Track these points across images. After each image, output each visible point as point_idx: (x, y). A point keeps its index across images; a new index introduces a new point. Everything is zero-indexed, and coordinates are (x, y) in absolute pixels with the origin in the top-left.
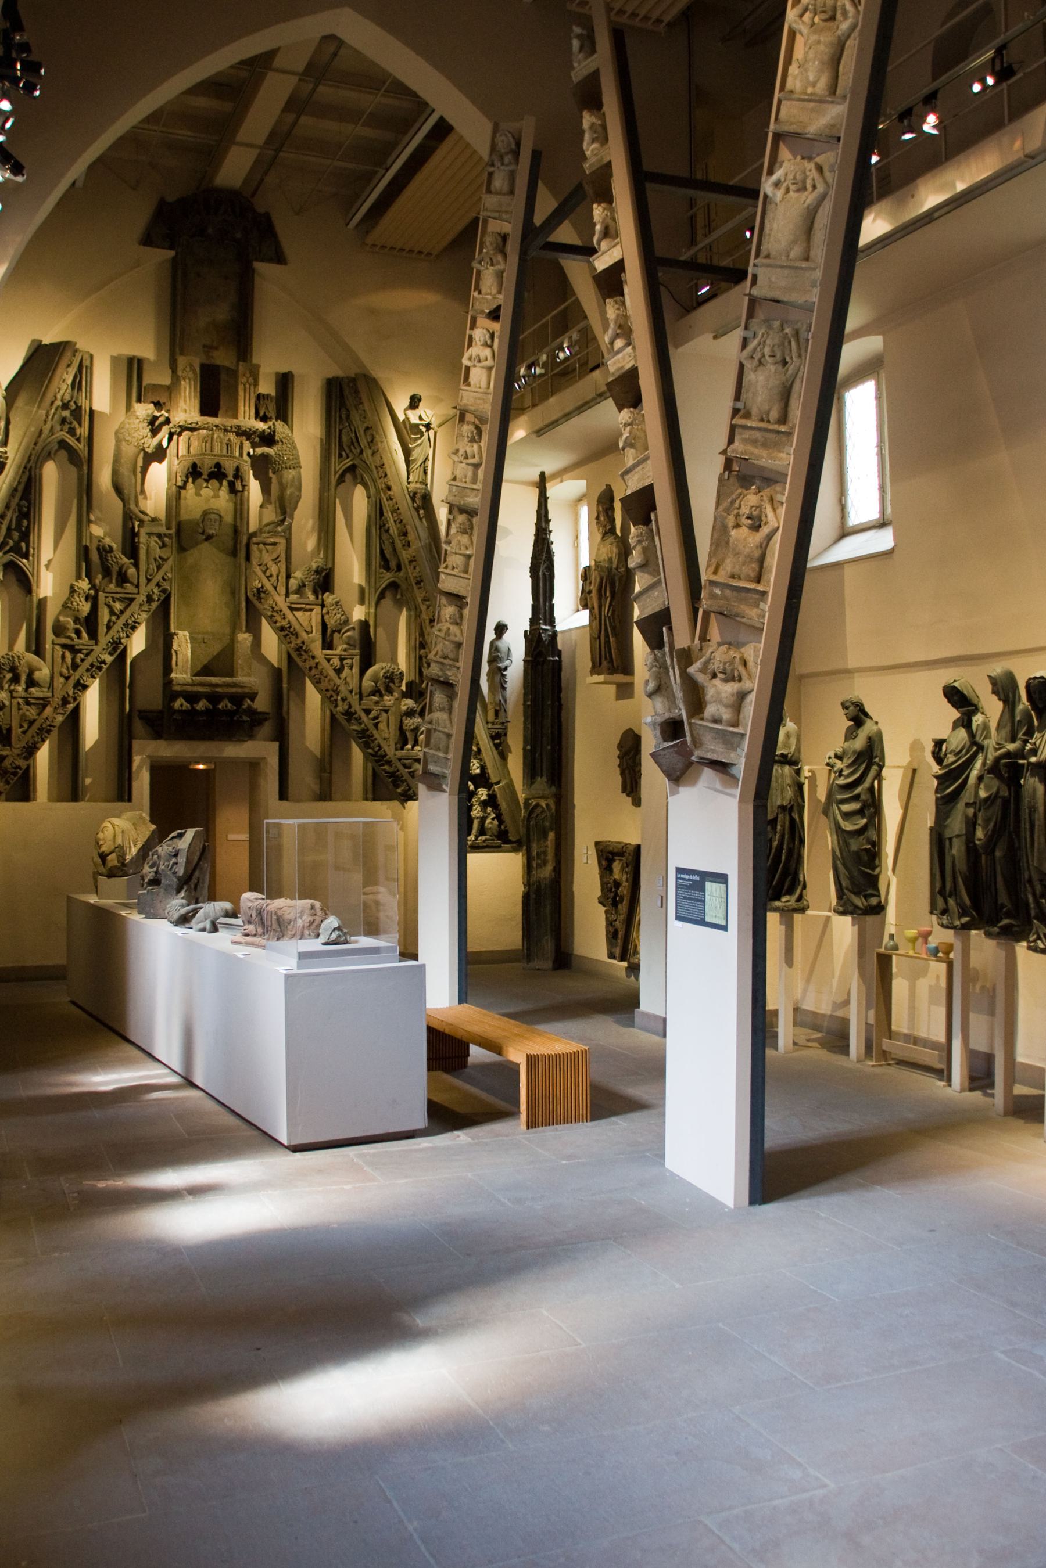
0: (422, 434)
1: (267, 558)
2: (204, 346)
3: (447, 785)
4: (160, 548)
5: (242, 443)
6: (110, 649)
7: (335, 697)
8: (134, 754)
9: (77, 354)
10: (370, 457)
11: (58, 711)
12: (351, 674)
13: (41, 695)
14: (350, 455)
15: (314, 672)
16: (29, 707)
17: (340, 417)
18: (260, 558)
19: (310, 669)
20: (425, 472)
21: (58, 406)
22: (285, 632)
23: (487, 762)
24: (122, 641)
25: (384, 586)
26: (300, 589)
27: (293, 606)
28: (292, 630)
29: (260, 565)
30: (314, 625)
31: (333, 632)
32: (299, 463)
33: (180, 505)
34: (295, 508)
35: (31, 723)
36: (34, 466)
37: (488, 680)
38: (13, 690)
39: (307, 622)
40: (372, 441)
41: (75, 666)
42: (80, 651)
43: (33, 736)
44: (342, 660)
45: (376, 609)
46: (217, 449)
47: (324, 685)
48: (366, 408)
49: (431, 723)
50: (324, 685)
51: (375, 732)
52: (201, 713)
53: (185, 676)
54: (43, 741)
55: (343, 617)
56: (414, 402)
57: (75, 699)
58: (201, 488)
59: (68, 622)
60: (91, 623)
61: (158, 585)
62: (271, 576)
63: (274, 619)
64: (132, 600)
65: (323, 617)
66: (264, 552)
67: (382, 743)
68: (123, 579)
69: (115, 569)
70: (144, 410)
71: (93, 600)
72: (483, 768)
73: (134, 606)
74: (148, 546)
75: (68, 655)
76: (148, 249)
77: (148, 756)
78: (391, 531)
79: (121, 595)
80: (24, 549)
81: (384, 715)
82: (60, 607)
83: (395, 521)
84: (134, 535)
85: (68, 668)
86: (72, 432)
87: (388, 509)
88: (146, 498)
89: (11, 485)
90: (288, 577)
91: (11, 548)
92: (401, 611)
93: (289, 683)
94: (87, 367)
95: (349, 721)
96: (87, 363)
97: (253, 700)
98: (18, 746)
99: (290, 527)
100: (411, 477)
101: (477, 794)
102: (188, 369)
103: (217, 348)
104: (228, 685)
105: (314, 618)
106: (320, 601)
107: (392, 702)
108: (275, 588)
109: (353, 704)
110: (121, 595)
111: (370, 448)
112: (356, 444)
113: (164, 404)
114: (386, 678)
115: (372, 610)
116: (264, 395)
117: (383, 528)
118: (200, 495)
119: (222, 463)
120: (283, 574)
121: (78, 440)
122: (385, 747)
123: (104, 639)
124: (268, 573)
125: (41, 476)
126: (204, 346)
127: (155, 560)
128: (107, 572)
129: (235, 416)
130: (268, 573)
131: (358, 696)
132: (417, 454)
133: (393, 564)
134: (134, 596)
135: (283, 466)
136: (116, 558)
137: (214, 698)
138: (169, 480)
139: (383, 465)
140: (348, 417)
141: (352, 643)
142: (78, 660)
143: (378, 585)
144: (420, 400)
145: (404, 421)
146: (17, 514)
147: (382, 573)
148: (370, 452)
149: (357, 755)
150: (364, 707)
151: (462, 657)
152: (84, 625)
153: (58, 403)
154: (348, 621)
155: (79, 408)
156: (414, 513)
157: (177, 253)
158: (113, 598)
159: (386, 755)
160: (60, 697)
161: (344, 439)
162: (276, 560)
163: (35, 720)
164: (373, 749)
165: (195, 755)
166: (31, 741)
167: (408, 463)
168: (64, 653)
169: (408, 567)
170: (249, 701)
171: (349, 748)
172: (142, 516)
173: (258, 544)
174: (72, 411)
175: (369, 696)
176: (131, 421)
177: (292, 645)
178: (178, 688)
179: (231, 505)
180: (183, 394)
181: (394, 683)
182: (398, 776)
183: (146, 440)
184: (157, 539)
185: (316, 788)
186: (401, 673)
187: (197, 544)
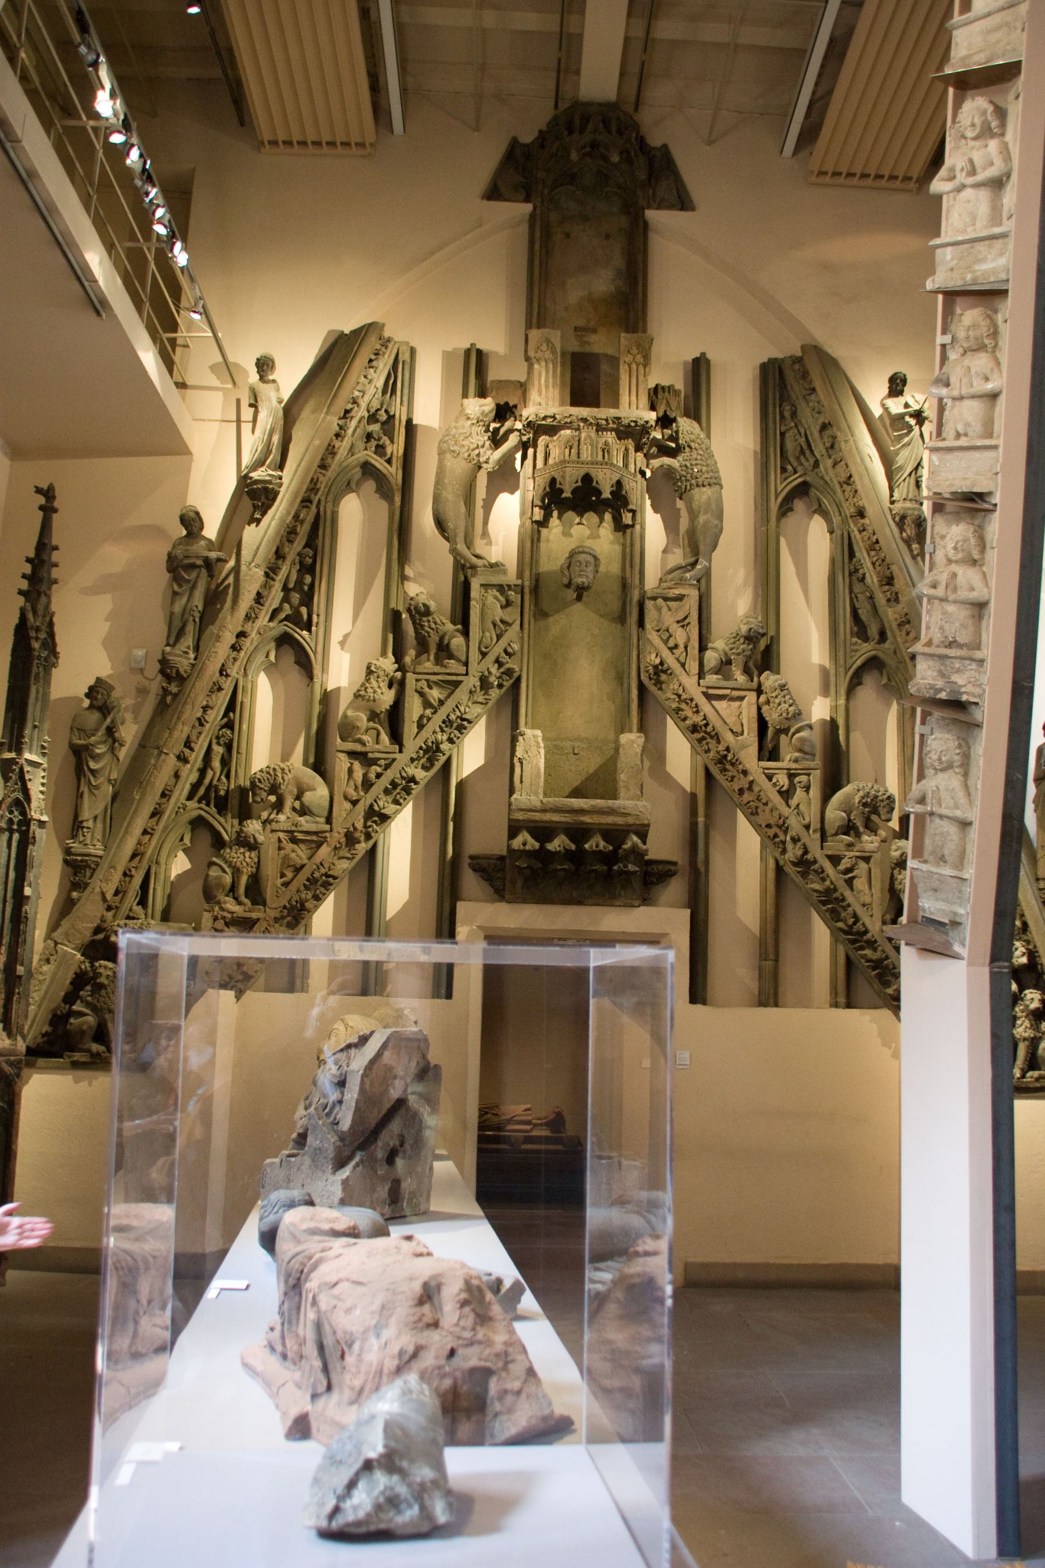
0: (910, 429)
1: (669, 619)
2: (576, 329)
3: (963, 944)
4: (502, 607)
5: (627, 450)
6: (423, 760)
7: (782, 837)
8: (458, 924)
9: (390, 346)
10: (831, 471)
11: (341, 853)
12: (807, 801)
13: (313, 827)
14: (800, 469)
15: (747, 797)
16: (295, 846)
17: (782, 417)
18: (659, 621)
19: (741, 792)
20: (918, 485)
21: (362, 418)
23: (1038, 944)
24: (443, 747)
25: (859, 663)
26: (724, 665)
27: (711, 691)
28: (709, 729)
29: (658, 631)
30: (745, 722)
31: (779, 732)
32: (718, 478)
33: (538, 548)
34: (714, 547)
35: (298, 869)
36: (323, 499)
37: (1035, 811)
38: (272, 820)
39: (734, 719)
40: (832, 447)
41: (367, 785)
42: (374, 762)
43: (298, 891)
44: (791, 776)
45: (848, 699)
46: (586, 455)
47: (764, 818)
48: (822, 397)
49: (922, 801)
50: (764, 818)
51: (847, 893)
53: (533, 798)
54: (318, 899)
55: (791, 709)
56: (897, 386)
57: (368, 836)
58: (571, 526)
59: (358, 719)
60: (394, 719)
61: (497, 661)
62: (676, 646)
63: (682, 714)
64: (457, 684)
65: (759, 709)
66: (665, 610)
67: (860, 912)
68: (444, 651)
69: (433, 640)
70: (480, 407)
71: (399, 685)
72: (1032, 954)
73: (461, 694)
74: (484, 605)
75: (357, 765)
76: (491, 203)
77: (478, 927)
78: (868, 580)
79: (440, 677)
80: (305, 617)
81: (862, 865)
82: (352, 696)
83: (874, 564)
84: (466, 586)
85: (356, 788)
86: (380, 450)
87: (861, 545)
88: (490, 543)
89: (282, 520)
90: (702, 648)
91: (287, 616)
92: (889, 706)
93: (707, 816)
94: (403, 362)
96: (405, 356)
97: (643, 837)
98: (274, 906)
99: (707, 573)
100: (896, 495)
101: (1022, 999)
102: (544, 347)
103: (594, 331)
104: (601, 812)
106: (755, 684)
107: (876, 844)
108: (683, 665)
109: (809, 844)
110: (440, 677)
111: (830, 457)
112: (807, 452)
113: (515, 406)
114: (865, 805)
115: (842, 701)
116: (663, 388)
117: (855, 575)
118: (570, 535)
119: (593, 475)
120: (695, 643)
121: (389, 461)
122: (866, 920)
123: (412, 743)
126: (576, 329)
127: (495, 625)
128: (422, 646)
129: (616, 405)
130: (671, 644)
131: (818, 835)
132: (904, 459)
133: (873, 631)
134: (459, 678)
135: (693, 482)
136: (436, 623)
137: (578, 833)
138: (522, 514)
139: (851, 476)
140: (794, 414)
141: (807, 749)
142: (372, 776)
143: (850, 662)
144: (904, 382)
145: (881, 416)
146: (298, 567)
147: (855, 644)
148: (829, 462)
149: (821, 933)
150: (830, 853)
151: (988, 637)
152: (387, 725)
153: (361, 412)
154: (800, 714)
155: (390, 418)
156: (903, 547)
157: (535, 208)
158: (427, 680)
159: (866, 932)
160: (343, 831)
161: (790, 445)
162: (683, 623)
163: (303, 866)
164: (844, 921)
165: (554, 927)
166: (296, 898)
167: (890, 475)
168: (352, 764)
169: (897, 632)
170: (635, 838)
171: (808, 921)
172: (474, 560)
173: (654, 598)
174: (383, 424)
175: (836, 834)
176: (460, 424)
177: (712, 754)
178: (519, 816)
179: (618, 548)
180: (536, 383)
181: (879, 815)
182: (887, 966)
183: (482, 451)
184: (498, 594)
185: (754, 986)
186: (889, 798)
187: (566, 605)
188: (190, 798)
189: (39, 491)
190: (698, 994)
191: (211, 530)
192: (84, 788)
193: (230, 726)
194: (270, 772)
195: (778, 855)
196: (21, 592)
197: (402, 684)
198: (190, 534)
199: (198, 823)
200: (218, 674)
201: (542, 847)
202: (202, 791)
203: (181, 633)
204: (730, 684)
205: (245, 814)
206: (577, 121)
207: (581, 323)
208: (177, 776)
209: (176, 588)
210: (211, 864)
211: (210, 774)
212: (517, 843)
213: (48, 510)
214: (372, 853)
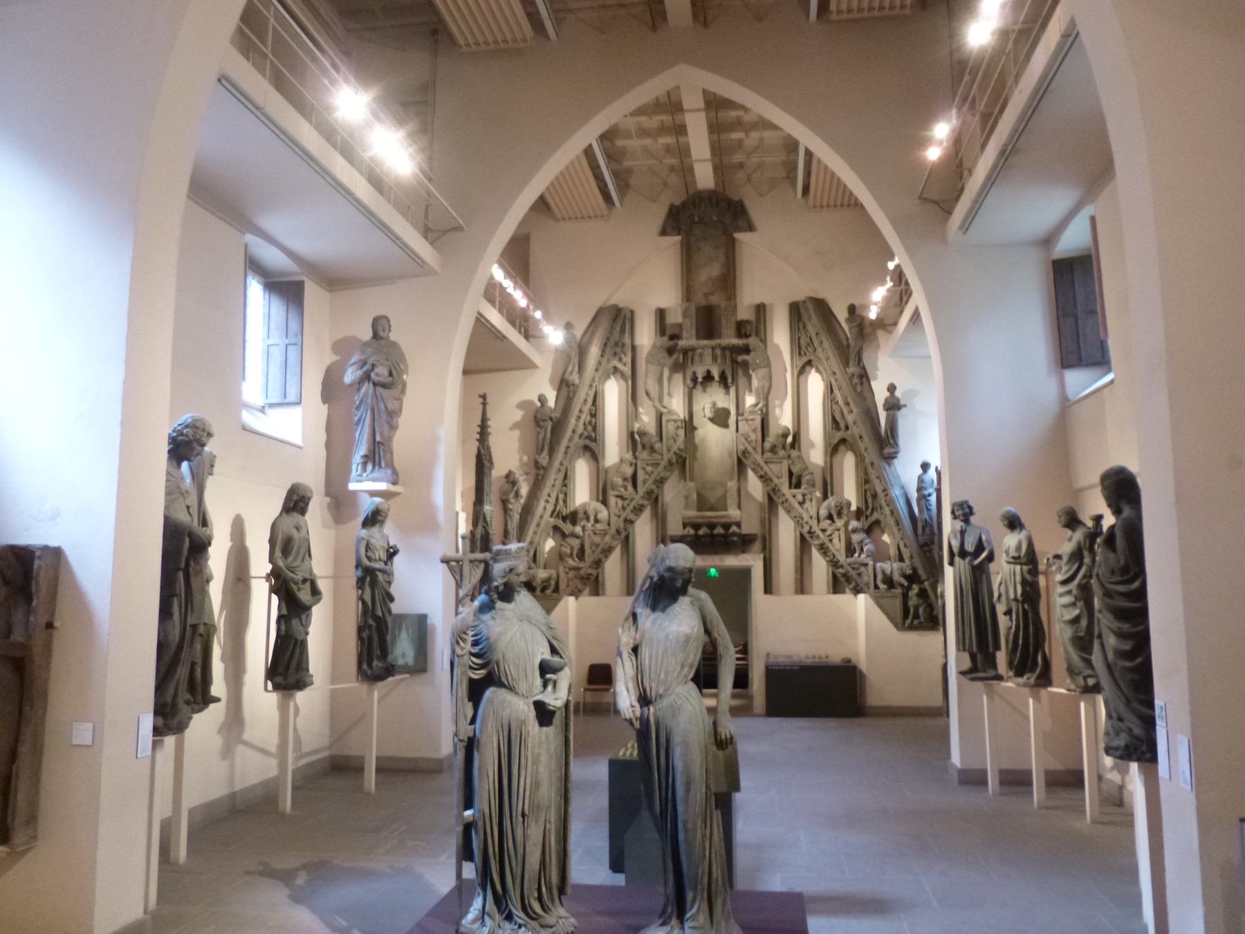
7: (801, 521)
14: (808, 354)
15: (786, 505)
17: (799, 329)
19: (783, 503)
22: (764, 478)
26: (773, 449)
27: (768, 460)
30: (783, 471)
35: (597, 546)
41: (624, 508)
44: (804, 495)
50: (793, 514)
51: (830, 546)
52: (702, 536)
54: (606, 557)
57: (626, 530)
64: (659, 464)
67: (836, 553)
68: (652, 450)
69: (648, 446)
73: (661, 468)
81: (837, 533)
85: (619, 511)
90: (763, 440)
95: (812, 537)
103: (712, 294)
105: (783, 468)
114: (837, 506)
115: (828, 460)
119: (711, 370)
121: (625, 365)
124: (749, 440)
125: (603, 390)
128: (644, 447)
130: (749, 440)
131: (816, 521)
133: (842, 425)
137: (712, 526)
140: (804, 327)
142: (625, 505)
157: (683, 238)
159: (839, 561)
161: (803, 342)
178: (687, 521)
188: (551, 516)
189: (480, 396)
190: (768, 589)
191: (551, 403)
192: (508, 518)
193: (565, 485)
194: (584, 505)
195: (800, 528)
196: (478, 440)
197: (636, 465)
198: (542, 405)
199: (556, 528)
200: (559, 466)
201: (696, 534)
202: (555, 514)
203: (542, 450)
204: (776, 456)
205: (574, 523)
206: (697, 200)
207: (706, 291)
208: (545, 508)
209: (539, 429)
210: (562, 545)
211: (558, 507)
212: (685, 532)
213: (484, 404)
214: (627, 537)
